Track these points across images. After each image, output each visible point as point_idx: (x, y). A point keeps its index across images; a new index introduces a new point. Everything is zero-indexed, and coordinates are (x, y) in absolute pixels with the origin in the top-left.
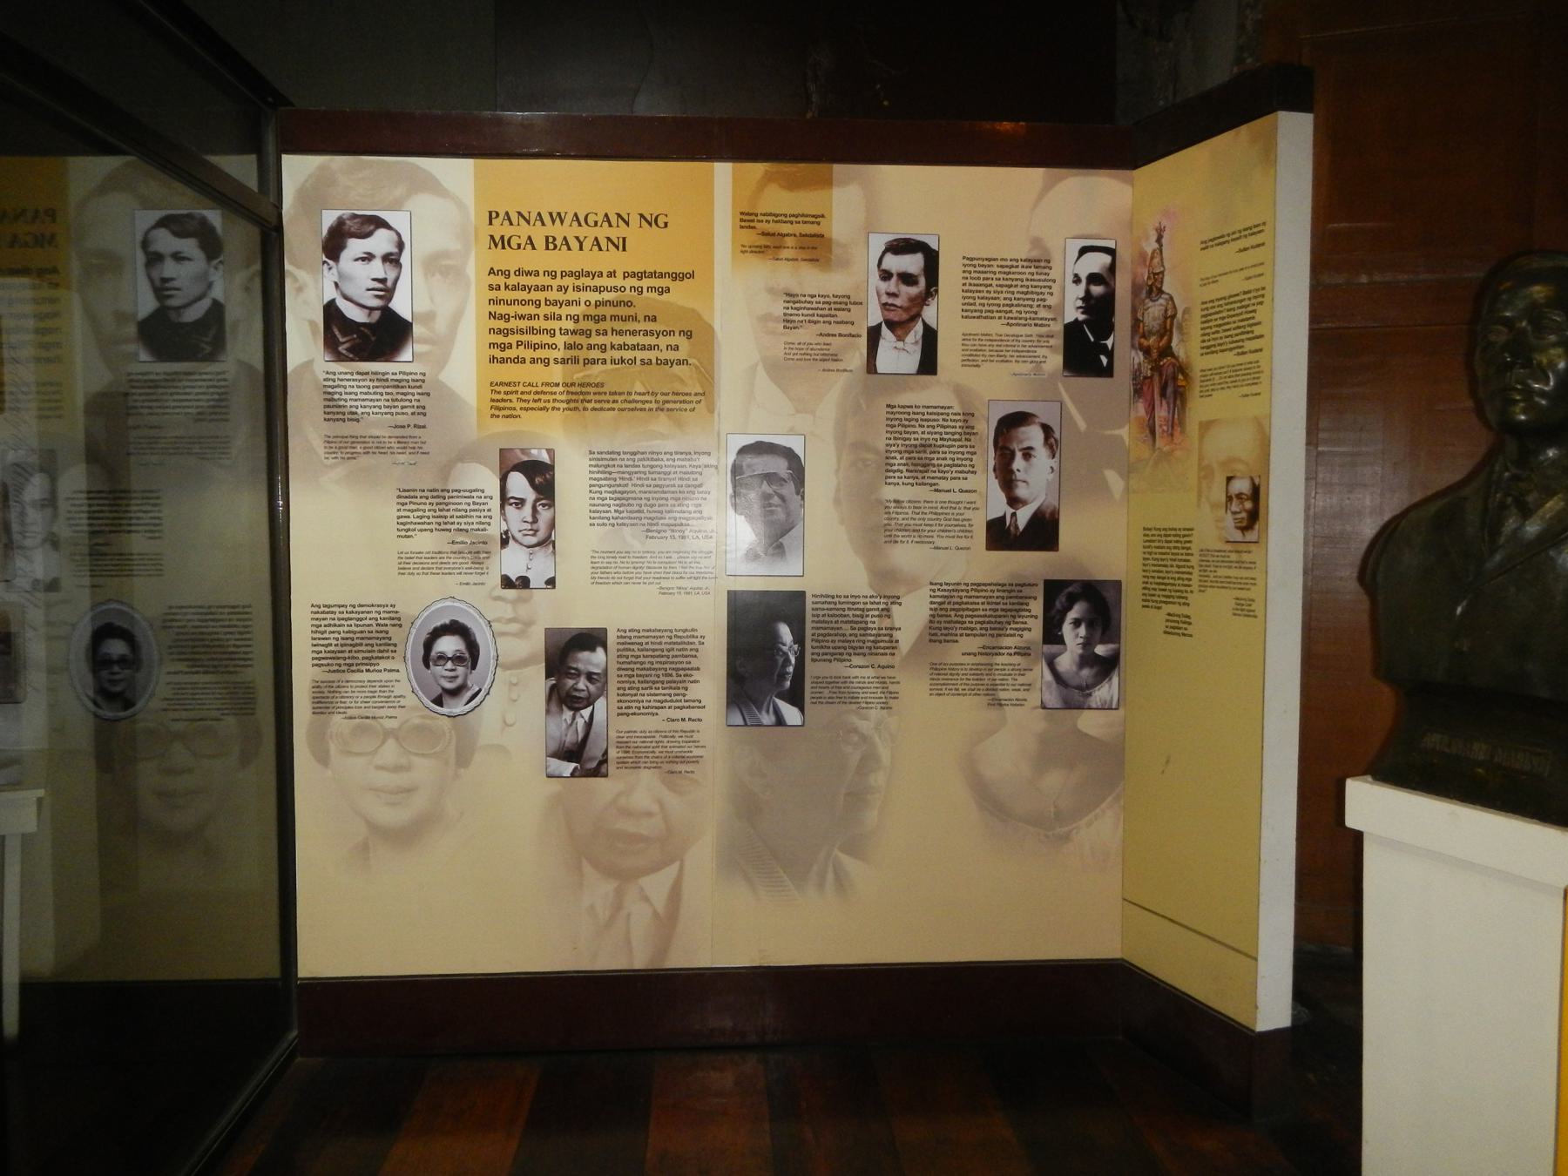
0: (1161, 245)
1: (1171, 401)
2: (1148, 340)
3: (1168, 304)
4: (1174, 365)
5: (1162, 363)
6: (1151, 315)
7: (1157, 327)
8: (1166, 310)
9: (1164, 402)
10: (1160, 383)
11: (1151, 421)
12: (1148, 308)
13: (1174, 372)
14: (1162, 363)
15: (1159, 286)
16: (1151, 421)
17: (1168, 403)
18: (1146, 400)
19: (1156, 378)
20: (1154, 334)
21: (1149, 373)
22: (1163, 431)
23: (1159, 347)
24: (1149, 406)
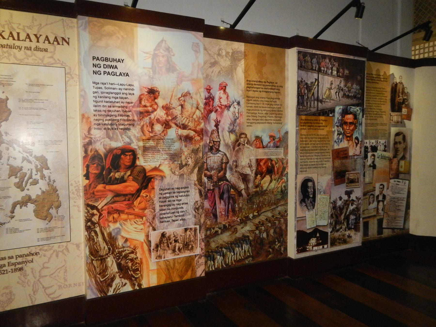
0: (218, 129)
1: (227, 201)
2: (211, 172)
3: (223, 157)
4: (228, 185)
5: (220, 184)
6: (212, 161)
7: (216, 166)
8: (222, 159)
9: (222, 201)
10: (219, 192)
11: (214, 210)
12: (210, 157)
13: (228, 187)
14: (220, 184)
15: (217, 147)
16: (214, 210)
17: (225, 202)
18: (210, 201)
19: (217, 190)
20: (214, 170)
21: (212, 188)
22: (222, 214)
23: (218, 176)
24: (212, 203)
